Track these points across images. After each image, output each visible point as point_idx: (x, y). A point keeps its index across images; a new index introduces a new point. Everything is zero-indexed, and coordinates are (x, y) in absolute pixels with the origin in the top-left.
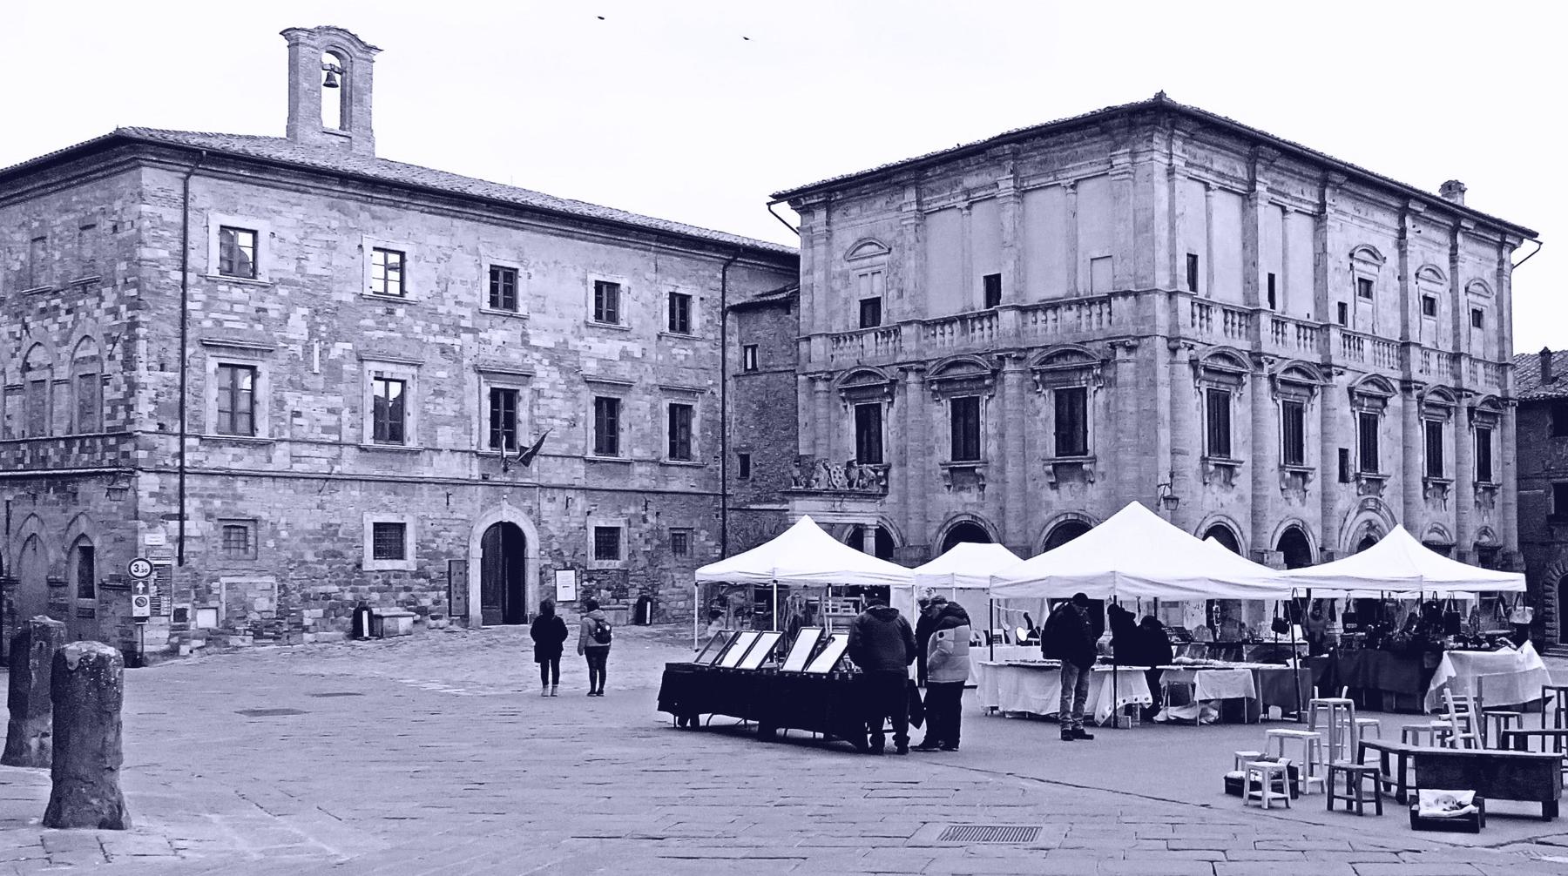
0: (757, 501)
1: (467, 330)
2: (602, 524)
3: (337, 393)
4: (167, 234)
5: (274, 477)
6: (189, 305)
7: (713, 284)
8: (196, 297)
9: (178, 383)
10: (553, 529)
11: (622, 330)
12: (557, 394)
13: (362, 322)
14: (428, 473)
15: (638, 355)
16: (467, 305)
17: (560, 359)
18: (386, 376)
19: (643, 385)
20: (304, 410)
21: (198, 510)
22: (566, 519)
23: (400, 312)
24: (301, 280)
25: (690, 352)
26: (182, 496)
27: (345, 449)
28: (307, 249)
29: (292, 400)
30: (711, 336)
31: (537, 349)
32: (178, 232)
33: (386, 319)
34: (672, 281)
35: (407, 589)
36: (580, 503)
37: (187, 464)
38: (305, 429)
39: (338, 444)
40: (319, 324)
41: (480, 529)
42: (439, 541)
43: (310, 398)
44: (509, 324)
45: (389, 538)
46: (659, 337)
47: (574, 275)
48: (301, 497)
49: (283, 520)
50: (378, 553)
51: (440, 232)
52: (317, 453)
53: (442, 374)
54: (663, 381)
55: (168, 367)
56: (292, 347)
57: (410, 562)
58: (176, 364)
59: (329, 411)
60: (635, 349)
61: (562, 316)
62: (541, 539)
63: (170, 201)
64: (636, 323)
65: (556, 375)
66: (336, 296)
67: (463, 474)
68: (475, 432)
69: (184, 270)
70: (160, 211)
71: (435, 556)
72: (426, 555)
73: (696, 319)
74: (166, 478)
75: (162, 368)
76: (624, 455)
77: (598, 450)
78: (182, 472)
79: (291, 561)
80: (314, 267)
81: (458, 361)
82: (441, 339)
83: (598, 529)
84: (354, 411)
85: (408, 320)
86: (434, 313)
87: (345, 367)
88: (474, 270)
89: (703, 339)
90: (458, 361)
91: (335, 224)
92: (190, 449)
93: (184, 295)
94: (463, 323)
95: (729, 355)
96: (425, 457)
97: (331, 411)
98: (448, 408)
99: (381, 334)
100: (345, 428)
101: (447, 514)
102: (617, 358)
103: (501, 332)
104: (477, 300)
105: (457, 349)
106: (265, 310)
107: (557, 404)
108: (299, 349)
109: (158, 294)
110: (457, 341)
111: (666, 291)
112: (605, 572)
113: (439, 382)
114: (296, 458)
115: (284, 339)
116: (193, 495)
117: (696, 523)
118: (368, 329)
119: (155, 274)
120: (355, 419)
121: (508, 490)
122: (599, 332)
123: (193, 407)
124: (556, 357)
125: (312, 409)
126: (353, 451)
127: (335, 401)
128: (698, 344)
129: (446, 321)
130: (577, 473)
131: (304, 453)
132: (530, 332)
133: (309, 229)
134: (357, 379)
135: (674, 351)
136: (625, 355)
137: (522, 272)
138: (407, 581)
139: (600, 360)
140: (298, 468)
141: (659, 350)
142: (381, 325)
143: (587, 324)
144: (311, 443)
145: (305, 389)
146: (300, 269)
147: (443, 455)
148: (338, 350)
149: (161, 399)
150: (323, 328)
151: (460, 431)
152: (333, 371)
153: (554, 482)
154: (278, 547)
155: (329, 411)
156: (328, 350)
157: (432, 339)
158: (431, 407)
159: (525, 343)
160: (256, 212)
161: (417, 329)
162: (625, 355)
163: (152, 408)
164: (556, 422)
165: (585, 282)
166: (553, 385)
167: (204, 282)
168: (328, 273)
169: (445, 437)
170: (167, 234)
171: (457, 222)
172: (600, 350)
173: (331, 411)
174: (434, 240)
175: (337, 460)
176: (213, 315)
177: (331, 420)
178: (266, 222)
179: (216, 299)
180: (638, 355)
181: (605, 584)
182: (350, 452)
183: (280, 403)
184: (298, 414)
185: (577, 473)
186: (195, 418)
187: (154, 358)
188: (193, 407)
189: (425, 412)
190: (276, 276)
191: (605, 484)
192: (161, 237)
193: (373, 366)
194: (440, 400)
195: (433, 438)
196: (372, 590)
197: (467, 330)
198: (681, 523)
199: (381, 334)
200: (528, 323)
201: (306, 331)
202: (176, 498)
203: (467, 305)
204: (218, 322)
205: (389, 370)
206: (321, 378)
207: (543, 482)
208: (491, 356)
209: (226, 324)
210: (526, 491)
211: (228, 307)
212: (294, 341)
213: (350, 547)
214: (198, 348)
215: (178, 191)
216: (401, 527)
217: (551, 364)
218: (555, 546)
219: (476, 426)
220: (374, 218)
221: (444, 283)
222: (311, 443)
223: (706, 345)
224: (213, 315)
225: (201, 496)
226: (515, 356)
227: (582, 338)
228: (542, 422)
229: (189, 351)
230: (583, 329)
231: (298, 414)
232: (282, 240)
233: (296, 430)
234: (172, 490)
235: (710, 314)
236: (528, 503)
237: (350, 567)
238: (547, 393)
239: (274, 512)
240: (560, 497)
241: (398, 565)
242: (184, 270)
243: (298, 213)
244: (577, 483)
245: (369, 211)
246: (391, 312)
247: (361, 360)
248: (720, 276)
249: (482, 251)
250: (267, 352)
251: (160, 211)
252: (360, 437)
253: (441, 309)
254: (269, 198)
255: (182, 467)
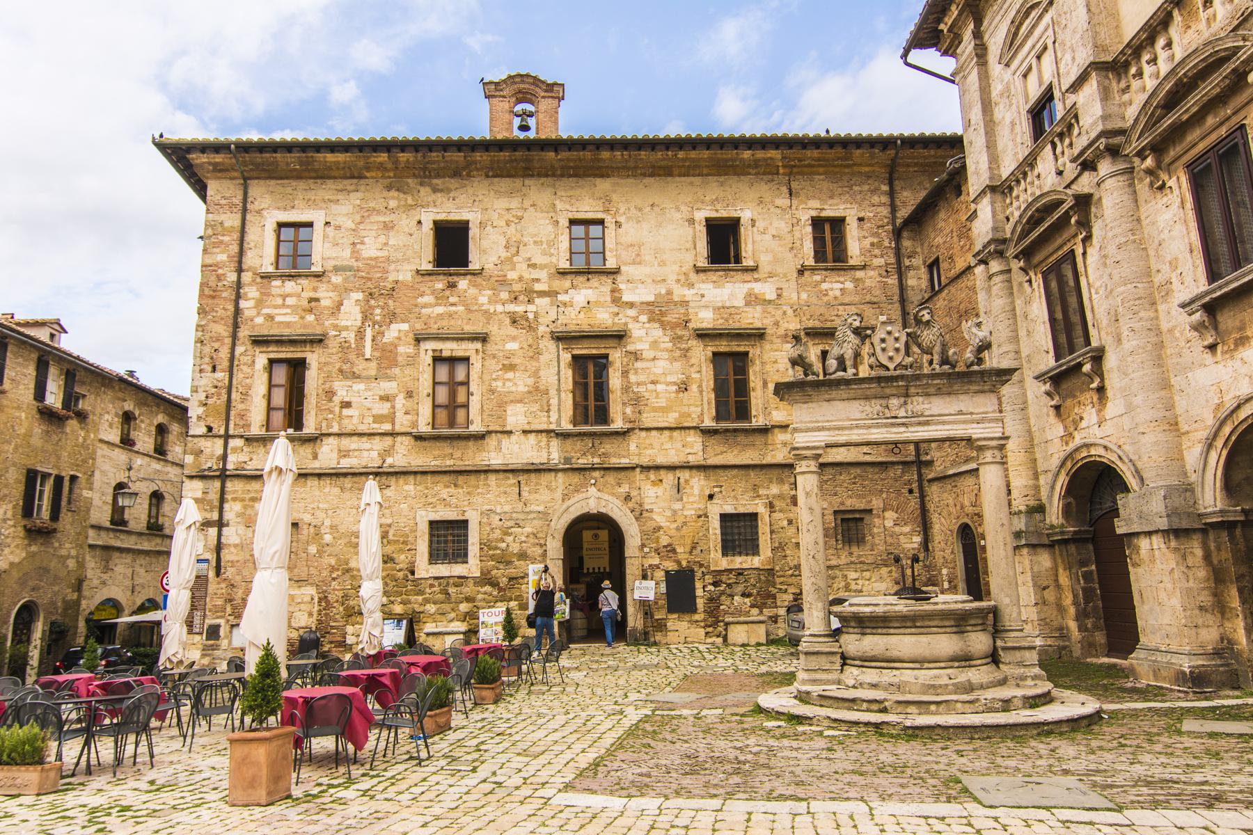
0: (954, 463)
1: (542, 294)
2: (729, 509)
3: (390, 378)
4: (226, 239)
5: (319, 476)
6: (243, 304)
7: (876, 199)
8: (250, 295)
9: (227, 382)
10: (660, 519)
11: (747, 270)
12: (659, 354)
13: (420, 300)
14: (496, 460)
15: (771, 295)
16: (542, 267)
17: (662, 314)
18: (446, 354)
19: (781, 331)
20: (353, 400)
21: (238, 515)
22: (677, 506)
23: (463, 284)
24: (355, 264)
25: (849, 285)
26: (222, 500)
27: (399, 439)
28: (363, 233)
29: (342, 390)
30: (881, 261)
31: (631, 305)
32: (236, 235)
33: (448, 293)
34: (815, 204)
35: (468, 599)
36: (697, 485)
37: (230, 466)
38: (355, 421)
39: (393, 434)
40: (372, 308)
41: (560, 524)
42: (509, 539)
43: (362, 386)
44: (595, 281)
45: (448, 538)
46: (801, 272)
47: (678, 215)
48: (347, 495)
49: (328, 523)
50: (435, 556)
51: (510, 194)
52: (367, 446)
53: (512, 346)
54: (811, 324)
55: (218, 367)
56: (344, 334)
57: (472, 567)
58: (226, 364)
59: (382, 398)
60: (767, 290)
61: (663, 263)
62: (642, 532)
63: (232, 206)
64: (765, 260)
65: (657, 332)
66: (392, 277)
67: (539, 458)
68: (554, 408)
69: (240, 270)
70: (222, 217)
71: (504, 560)
72: (492, 557)
73: (855, 244)
74: (210, 482)
75: (214, 369)
76: (758, 421)
77: (718, 418)
78: (223, 476)
79: (333, 569)
80: (370, 250)
81: (531, 328)
82: (512, 308)
83: (725, 518)
84: (410, 395)
85: (473, 291)
86: (503, 282)
87: (401, 349)
88: (550, 228)
89: (864, 267)
90: (531, 328)
91: (393, 204)
92: (235, 450)
93: (238, 297)
94: (538, 287)
95: (911, 282)
96: (492, 441)
97: (385, 398)
98: (519, 383)
99: (440, 310)
100: (399, 415)
101: (520, 506)
102: (740, 302)
103: (584, 292)
104: (554, 260)
105: (531, 316)
106: (317, 300)
107: (661, 366)
108: (351, 336)
109: (213, 297)
110: (531, 308)
111: (805, 216)
112: (740, 573)
113: (512, 354)
114: (344, 454)
115: (335, 327)
116: (234, 499)
117: (877, 503)
118: (425, 306)
119: (213, 278)
120: (410, 404)
121: (596, 474)
122: (713, 276)
123: (241, 406)
124: (656, 312)
125: (363, 400)
126: (407, 440)
127: (388, 387)
128: (860, 274)
129: (517, 287)
130: (693, 448)
131: (353, 446)
132: (622, 286)
133: (366, 213)
134: (412, 361)
135: (824, 286)
136: (753, 300)
137: (609, 221)
138: (469, 589)
139: (717, 309)
140: (346, 463)
141: (800, 287)
142: (440, 299)
143: (698, 270)
144: (361, 435)
145: (356, 376)
146: (356, 255)
147: (514, 438)
148: (394, 331)
149: (210, 401)
150: (378, 311)
151: (535, 407)
152: (387, 357)
153: (660, 460)
154: (320, 553)
155: (382, 398)
156: (383, 334)
157: (500, 308)
158: (499, 384)
159: (616, 300)
160: (312, 204)
161: (483, 300)
162: (753, 300)
163: (201, 410)
164: (660, 387)
165: (691, 221)
166: (654, 344)
167: (259, 280)
168: (385, 253)
169: (516, 417)
170: (226, 239)
171: (527, 182)
172: (717, 299)
173: (385, 398)
174: (502, 203)
175: (388, 452)
176: (265, 311)
177: (384, 408)
178: (322, 213)
179: (269, 294)
180: (773, 296)
181: (740, 588)
182: (403, 444)
183: (330, 394)
184: (347, 405)
185: (693, 448)
186: (242, 416)
187: (207, 360)
188: (241, 406)
189: (492, 391)
190: (330, 265)
191: (732, 458)
192: (221, 242)
193: (430, 345)
194: (510, 375)
195: (502, 418)
196: (427, 601)
197: (542, 294)
198: (852, 503)
199: (440, 310)
200: (619, 278)
201: (359, 317)
202: (217, 503)
203: (542, 267)
204: (270, 318)
205: (448, 348)
206: (374, 364)
207: (645, 461)
208: (574, 320)
209: (278, 319)
210: (622, 475)
211: (280, 301)
212: (346, 328)
213: (401, 551)
214: (249, 347)
215: (238, 200)
216: (464, 524)
217: (650, 321)
218: (664, 541)
219: (554, 402)
220: (435, 190)
221: (514, 247)
222: (361, 435)
223: (871, 273)
224: (265, 311)
225: (243, 500)
226: (604, 318)
227: (691, 285)
228: (642, 389)
229: (239, 350)
230: (693, 277)
231: (347, 405)
232: (338, 228)
233: (346, 421)
234: (214, 496)
235: (876, 235)
236: (624, 489)
237: (401, 575)
238: (648, 354)
239: (318, 513)
240: (669, 478)
241: (458, 570)
242: (240, 270)
243: (356, 198)
244: (692, 460)
245: (430, 185)
246: (452, 286)
247: (418, 340)
248: (885, 188)
249: (559, 205)
250: (318, 341)
251: (222, 217)
252: (415, 424)
253: (512, 275)
254: (326, 190)
255: (224, 469)
